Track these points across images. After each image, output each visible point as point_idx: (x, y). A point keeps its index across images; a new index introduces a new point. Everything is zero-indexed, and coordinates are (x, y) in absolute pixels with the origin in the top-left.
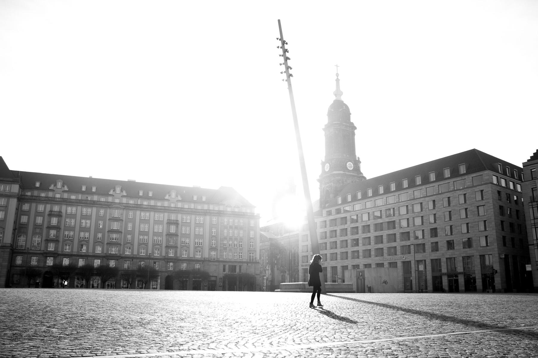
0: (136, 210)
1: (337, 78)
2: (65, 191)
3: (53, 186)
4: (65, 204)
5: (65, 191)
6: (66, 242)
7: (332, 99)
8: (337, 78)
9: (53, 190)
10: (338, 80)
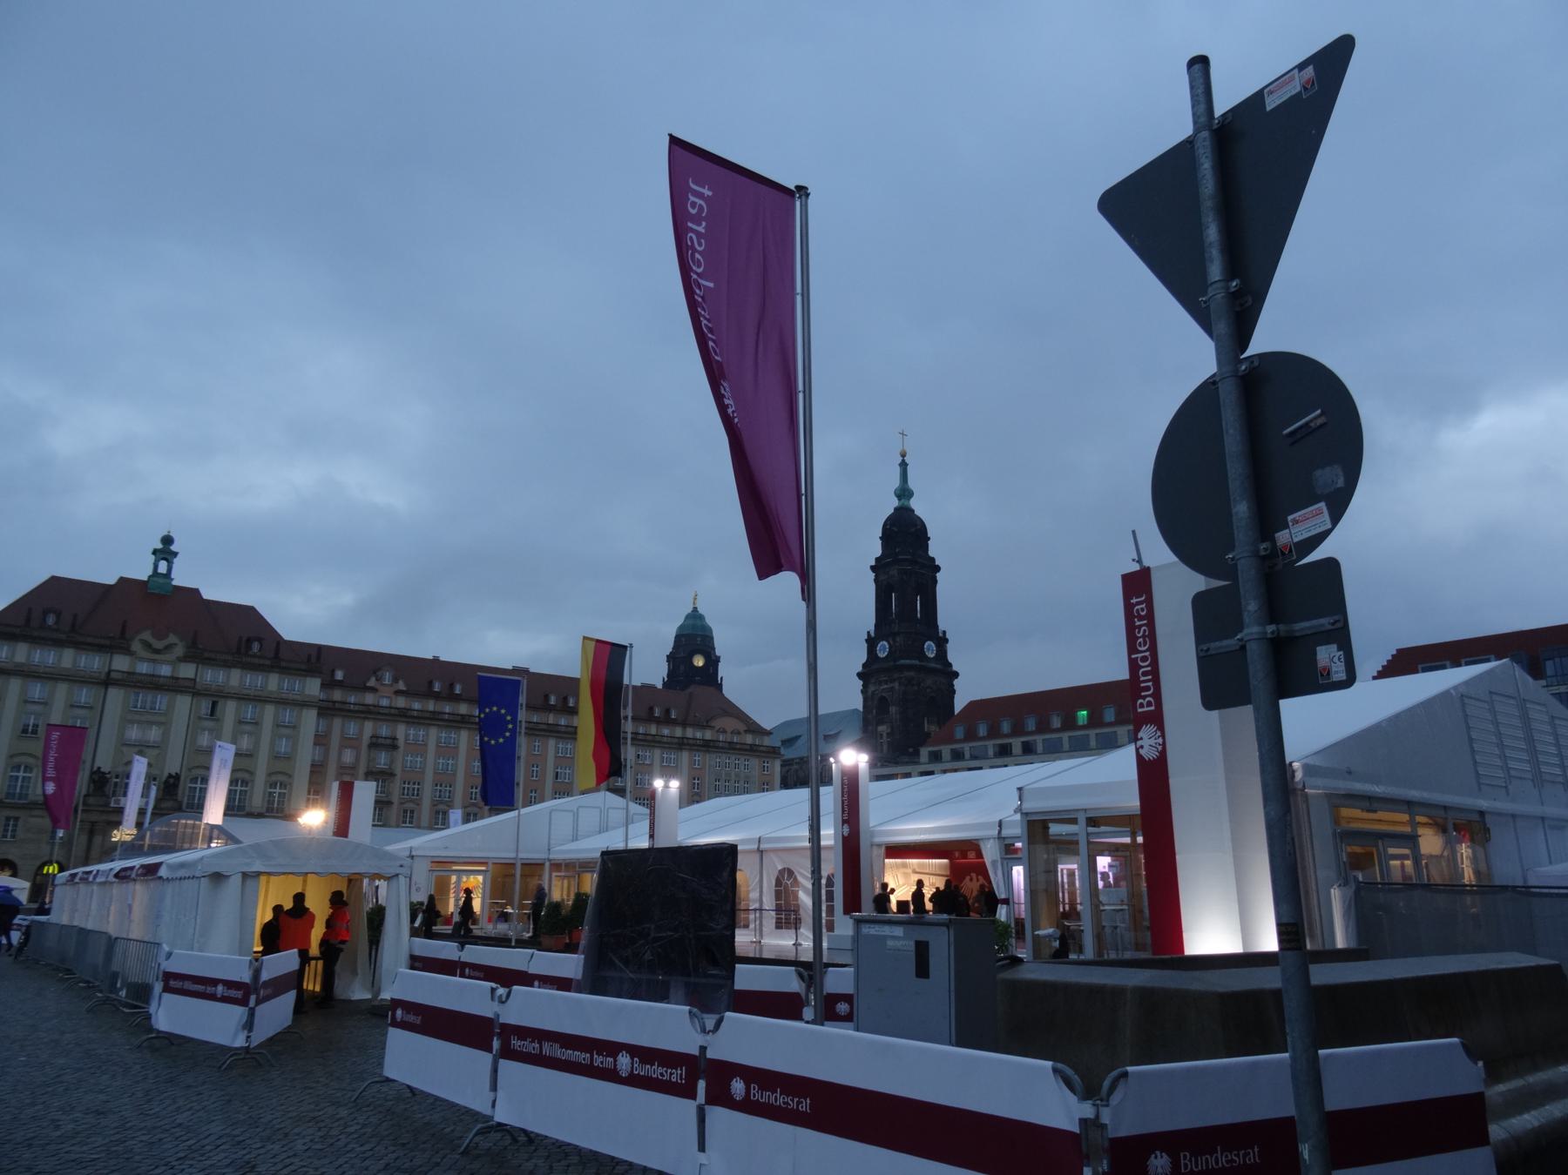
0: (548, 736)
1: (903, 461)
2: (398, 693)
3: (373, 679)
4: (403, 722)
5: (398, 693)
6: (405, 806)
7: (890, 504)
8: (903, 461)
9: (373, 690)
10: (904, 465)
